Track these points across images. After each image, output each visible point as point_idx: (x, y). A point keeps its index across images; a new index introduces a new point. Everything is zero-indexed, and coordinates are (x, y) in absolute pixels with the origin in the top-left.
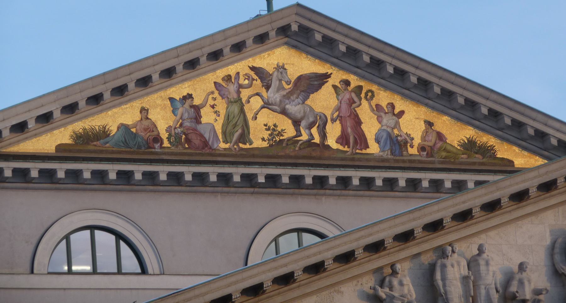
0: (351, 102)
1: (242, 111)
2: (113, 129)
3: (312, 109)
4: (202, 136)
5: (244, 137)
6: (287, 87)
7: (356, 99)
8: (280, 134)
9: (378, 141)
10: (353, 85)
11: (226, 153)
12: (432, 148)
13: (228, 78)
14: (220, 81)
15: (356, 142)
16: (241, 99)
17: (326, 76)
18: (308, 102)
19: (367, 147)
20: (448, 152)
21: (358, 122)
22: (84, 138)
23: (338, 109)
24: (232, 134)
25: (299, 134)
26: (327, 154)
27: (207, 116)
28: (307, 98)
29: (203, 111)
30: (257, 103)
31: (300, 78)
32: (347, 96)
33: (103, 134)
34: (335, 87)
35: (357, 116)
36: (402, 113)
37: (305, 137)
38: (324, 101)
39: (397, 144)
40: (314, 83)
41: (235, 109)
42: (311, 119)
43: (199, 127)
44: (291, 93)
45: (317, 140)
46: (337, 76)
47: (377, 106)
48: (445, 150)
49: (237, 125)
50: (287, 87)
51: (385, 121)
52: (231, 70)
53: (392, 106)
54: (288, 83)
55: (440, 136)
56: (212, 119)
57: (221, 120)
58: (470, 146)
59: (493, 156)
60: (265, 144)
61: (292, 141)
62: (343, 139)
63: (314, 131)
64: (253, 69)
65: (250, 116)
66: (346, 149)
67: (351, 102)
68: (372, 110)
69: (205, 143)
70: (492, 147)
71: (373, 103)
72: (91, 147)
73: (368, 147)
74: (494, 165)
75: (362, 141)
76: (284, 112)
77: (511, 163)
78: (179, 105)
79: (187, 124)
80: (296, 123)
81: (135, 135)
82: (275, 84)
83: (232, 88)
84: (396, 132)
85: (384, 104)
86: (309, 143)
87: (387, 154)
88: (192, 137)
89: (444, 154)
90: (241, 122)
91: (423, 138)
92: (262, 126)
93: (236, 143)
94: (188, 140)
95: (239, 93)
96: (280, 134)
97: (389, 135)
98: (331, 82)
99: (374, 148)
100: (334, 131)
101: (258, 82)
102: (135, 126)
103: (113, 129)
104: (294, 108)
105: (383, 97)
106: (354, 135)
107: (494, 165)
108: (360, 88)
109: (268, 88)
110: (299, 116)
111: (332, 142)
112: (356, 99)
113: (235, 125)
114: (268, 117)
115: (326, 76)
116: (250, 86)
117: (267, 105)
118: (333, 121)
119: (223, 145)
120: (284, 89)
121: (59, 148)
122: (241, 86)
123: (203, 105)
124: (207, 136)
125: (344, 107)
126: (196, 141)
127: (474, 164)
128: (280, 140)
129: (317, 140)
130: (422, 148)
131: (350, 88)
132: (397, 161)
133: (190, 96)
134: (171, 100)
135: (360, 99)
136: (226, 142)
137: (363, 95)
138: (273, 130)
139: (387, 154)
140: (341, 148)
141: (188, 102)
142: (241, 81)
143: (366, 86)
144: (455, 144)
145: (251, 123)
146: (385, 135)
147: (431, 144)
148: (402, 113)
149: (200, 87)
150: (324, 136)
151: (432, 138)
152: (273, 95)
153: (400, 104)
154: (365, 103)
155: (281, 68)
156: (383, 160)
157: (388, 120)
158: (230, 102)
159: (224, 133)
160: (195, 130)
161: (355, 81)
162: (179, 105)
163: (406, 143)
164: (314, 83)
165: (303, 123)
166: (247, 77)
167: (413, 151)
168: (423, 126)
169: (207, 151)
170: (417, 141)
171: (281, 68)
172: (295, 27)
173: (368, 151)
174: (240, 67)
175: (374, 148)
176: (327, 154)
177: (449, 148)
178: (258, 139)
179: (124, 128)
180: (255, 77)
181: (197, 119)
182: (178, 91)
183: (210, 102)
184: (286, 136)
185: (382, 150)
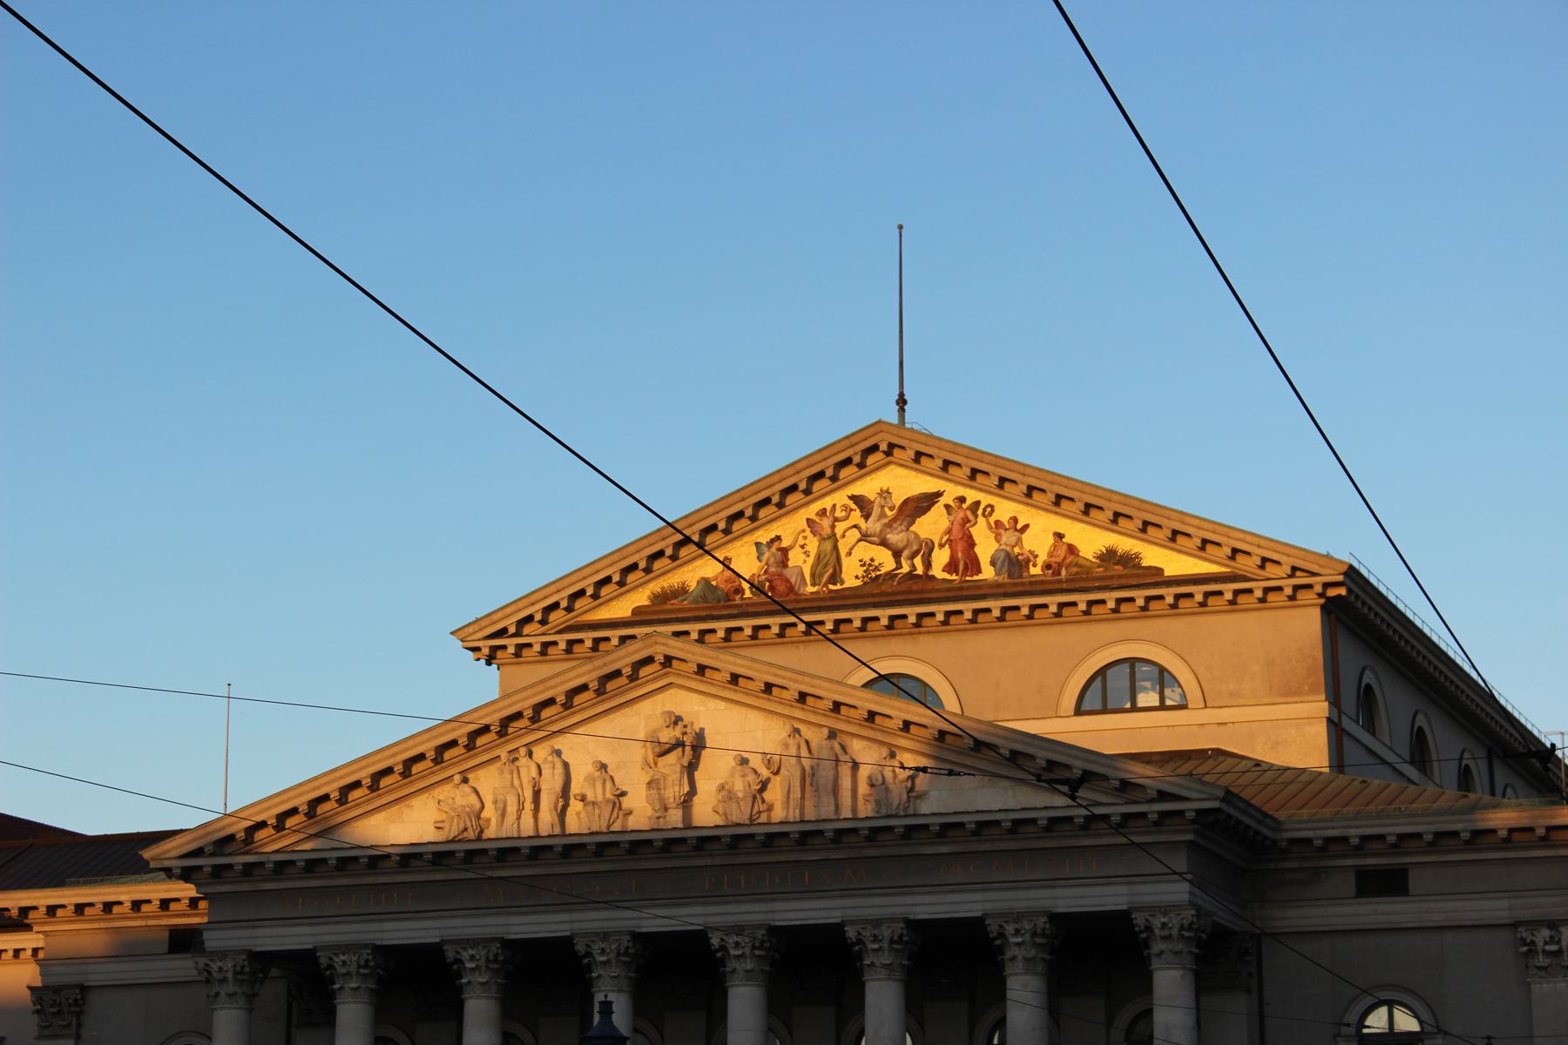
0: (966, 521)
1: (836, 548)
2: (693, 585)
3: (917, 536)
4: (788, 581)
5: (835, 577)
6: (889, 513)
7: (971, 517)
8: (877, 569)
9: (993, 563)
10: (968, 503)
11: (814, 597)
12: (1060, 565)
13: (823, 512)
14: (813, 516)
15: (966, 568)
16: (834, 535)
17: (939, 494)
18: (912, 528)
19: (979, 571)
20: (1080, 566)
21: (971, 543)
22: (661, 598)
23: (949, 531)
24: (822, 575)
25: (899, 566)
26: (930, 585)
27: (796, 558)
28: (912, 523)
29: (791, 554)
30: (855, 534)
31: (906, 502)
32: (961, 515)
33: (682, 591)
34: (947, 507)
35: (970, 537)
36: (1026, 526)
37: (906, 569)
38: (932, 525)
39: (1014, 564)
40: (925, 503)
41: (828, 546)
42: (915, 548)
43: (786, 572)
44: (894, 520)
45: (920, 571)
46: (951, 491)
47: (997, 522)
48: (1077, 565)
49: (829, 565)
50: (889, 513)
51: (1004, 539)
52: (826, 503)
53: (1015, 520)
54: (892, 509)
55: (1072, 549)
56: (801, 562)
57: (811, 561)
58: (1109, 556)
59: (1139, 566)
60: (859, 583)
61: (891, 575)
62: (951, 567)
63: (918, 561)
64: (852, 498)
65: (843, 552)
66: (954, 577)
67: (966, 521)
68: (990, 528)
69: (791, 589)
70: (1137, 556)
71: (992, 520)
72: (667, 607)
73: (979, 571)
74: (1138, 576)
75: (974, 565)
76: (884, 543)
77: (1160, 571)
78: (765, 549)
79: (772, 569)
80: (897, 555)
81: (716, 588)
82: (876, 511)
83: (826, 523)
84: (1017, 550)
85: (1005, 520)
86: (911, 575)
87: (1003, 578)
88: (777, 583)
89: (1075, 570)
90: (833, 561)
91: (1050, 555)
92: (859, 561)
93: (826, 585)
94: (772, 588)
95: (833, 527)
96: (877, 569)
97: (1008, 555)
98: (943, 500)
99: (988, 573)
100: (941, 557)
101: (858, 513)
102: (716, 578)
103: (693, 585)
104: (895, 538)
105: (1005, 510)
106: (966, 560)
107: (1138, 576)
108: (978, 503)
109: (867, 517)
110: (901, 545)
111: (937, 571)
112: (971, 517)
113: (826, 565)
114: (867, 551)
115: (939, 494)
116: (847, 518)
117: (865, 537)
118: (941, 546)
119: (810, 589)
120: (885, 516)
121: (636, 611)
122: (836, 520)
123: (791, 547)
124: (793, 581)
125: (956, 528)
126: (781, 588)
127: (1112, 577)
128: (878, 577)
129: (920, 571)
130: (1047, 566)
131: (965, 506)
132: (1015, 585)
133: (778, 538)
134: (758, 545)
135: (976, 516)
136: (813, 585)
137: (980, 512)
138: (869, 566)
139: (1003, 578)
140: (947, 576)
141: (776, 544)
142: (839, 514)
143: (986, 500)
144: (1090, 556)
145: (845, 561)
146: (1002, 556)
147: (1059, 560)
148: (1026, 526)
149: (789, 527)
150: (928, 564)
151: (1062, 552)
152: (873, 525)
153: (1025, 515)
154: (981, 519)
155: (885, 494)
156: (997, 585)
157: (1009, 537)
158: (822, 540)
159: (813, 575)
160: (780, 575)
161: (972, 495)
162: (765, 549)
163: (1028, 561)
164: (925, 503)
165: (906, 553)
166: (846, 508)
167: (1035, 571)
168: (1051, 540)
169: (792, 597)
170: (1040, 561)
171: (885, 494)
172: (883, 447)
173: (980, 577)
174: (840, 498)
175: (988, 573)
176: (930, 585)
177: (1081, 561)
178: (851, 577)
179: (705, 582)
180: (854, 506)
181: (784, 563)
182: (763, 536)
183: (801, 541)
184: (883, 571)
185: (998, 573)
